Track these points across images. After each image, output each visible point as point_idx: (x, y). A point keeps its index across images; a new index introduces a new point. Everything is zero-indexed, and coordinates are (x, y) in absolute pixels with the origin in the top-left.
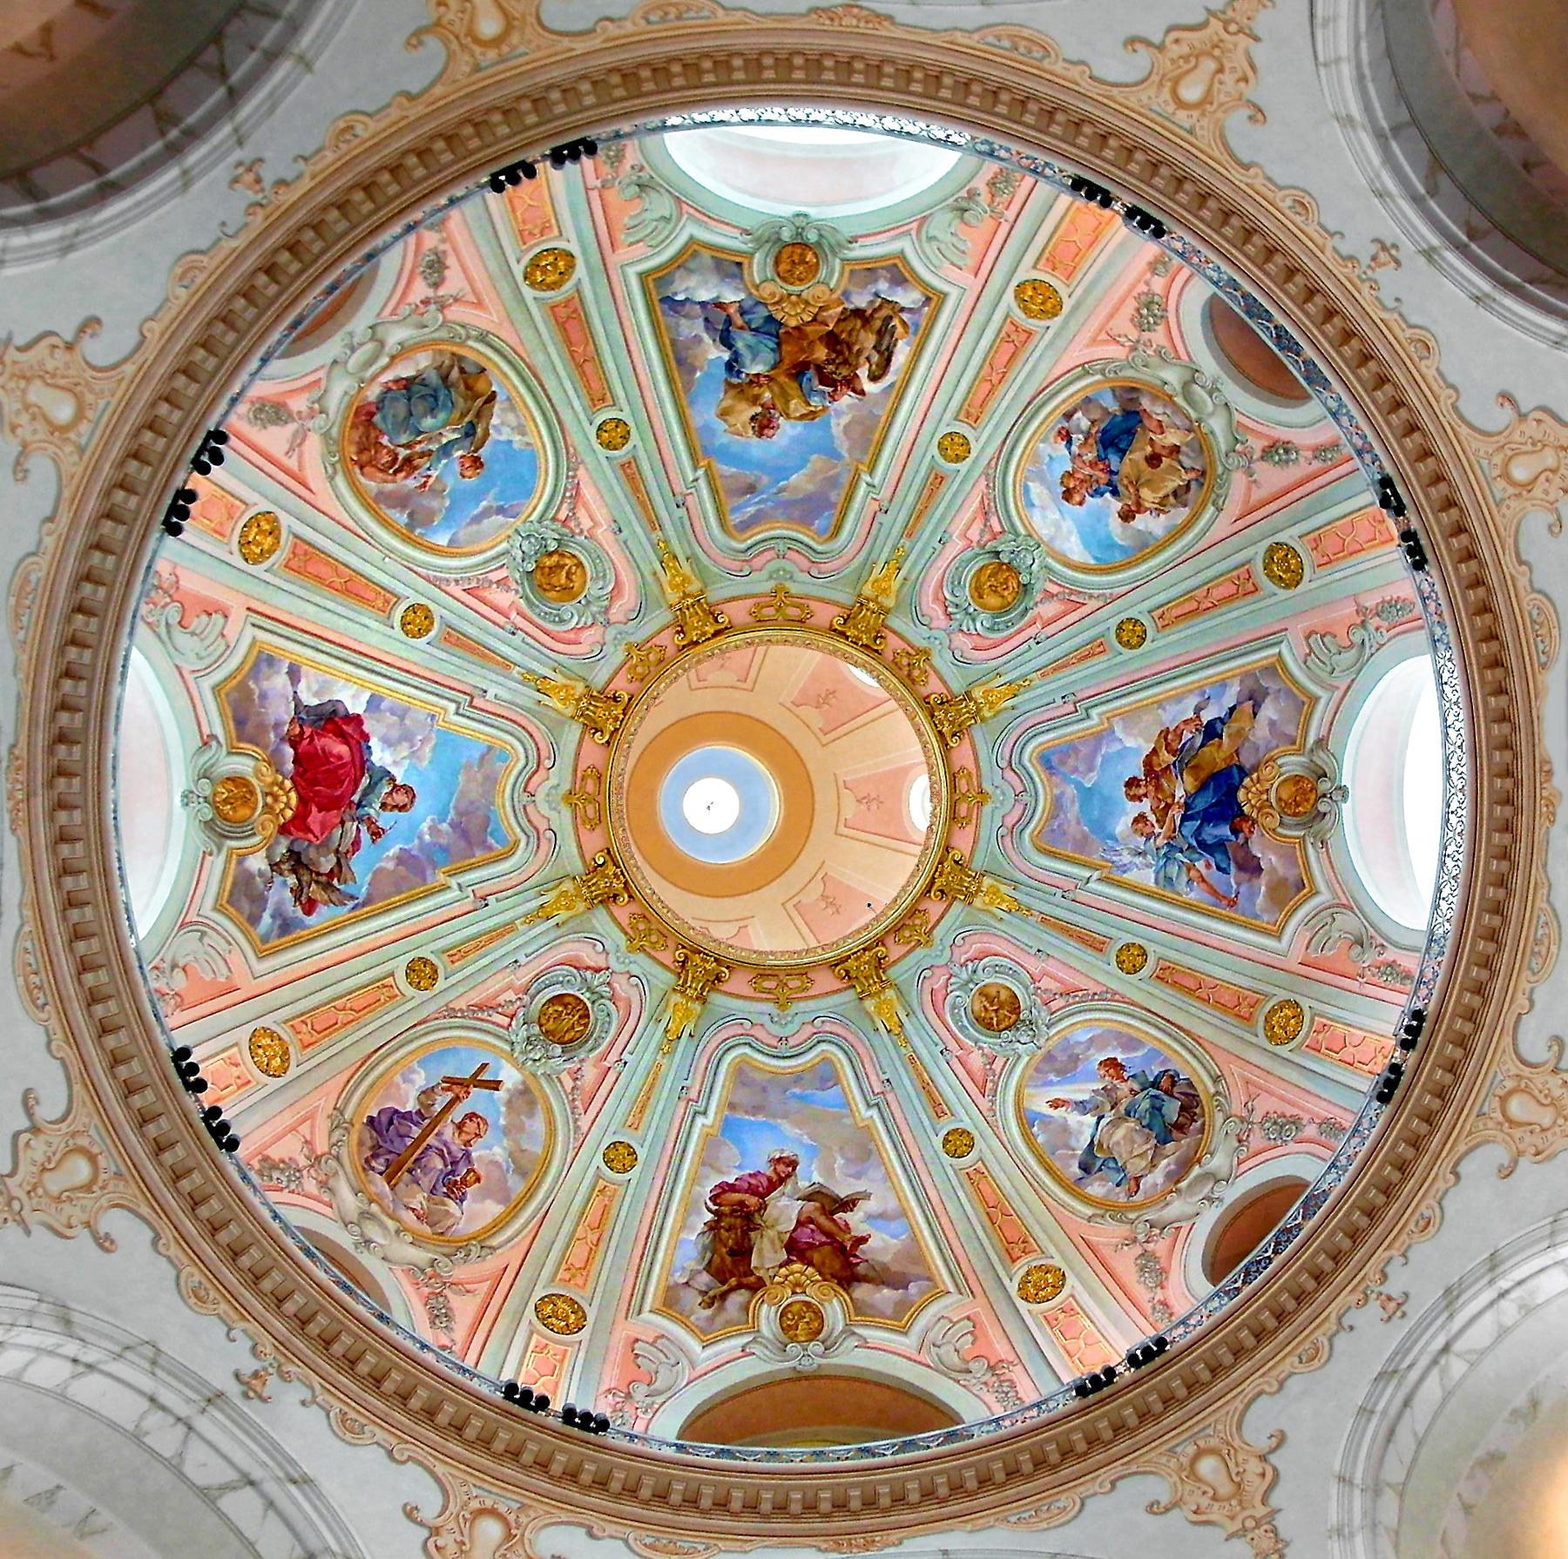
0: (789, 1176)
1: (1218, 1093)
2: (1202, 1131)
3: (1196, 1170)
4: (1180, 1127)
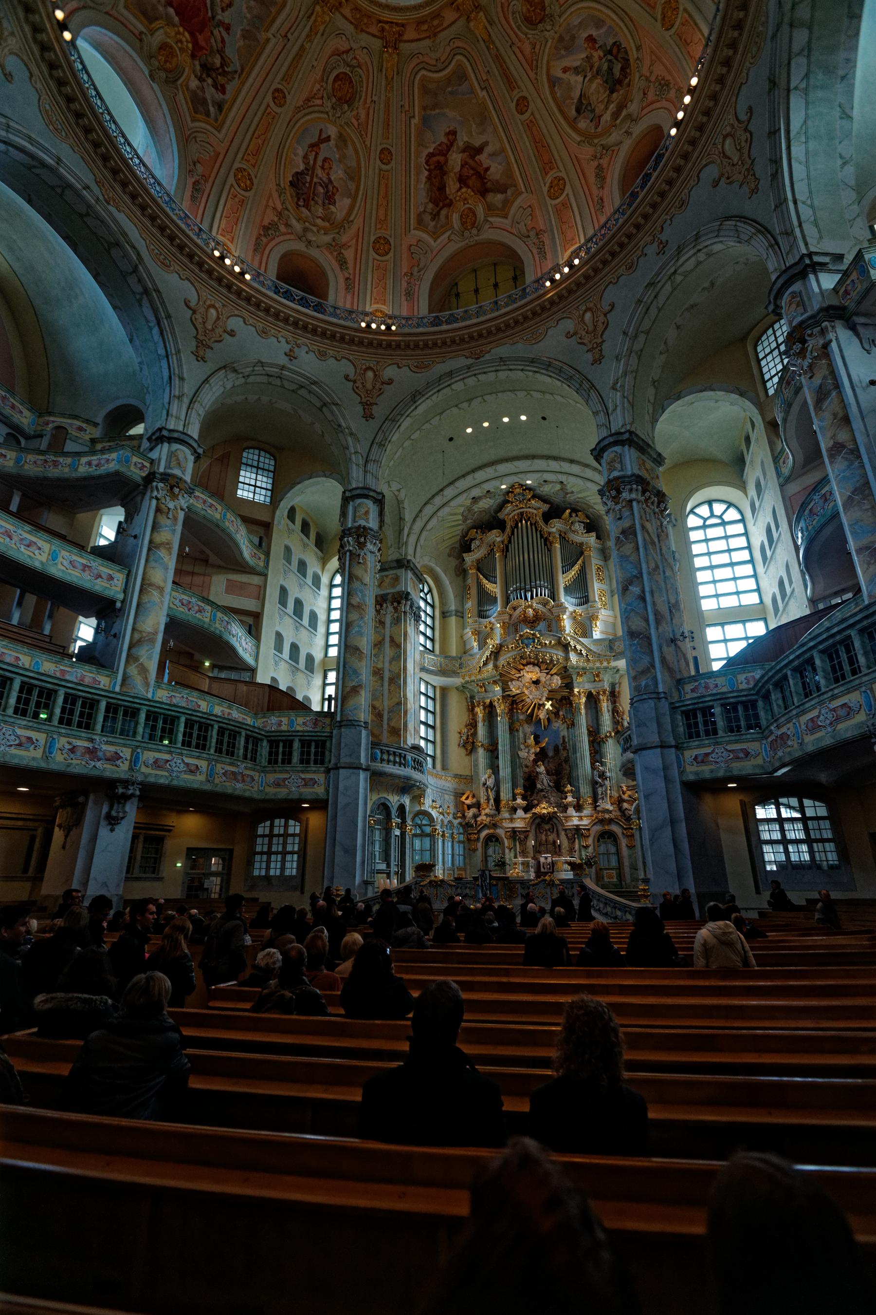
0: (455, 140)
1: (638, 59)
2: (629, 85)
3: (624, 113)
4: (620, 82)
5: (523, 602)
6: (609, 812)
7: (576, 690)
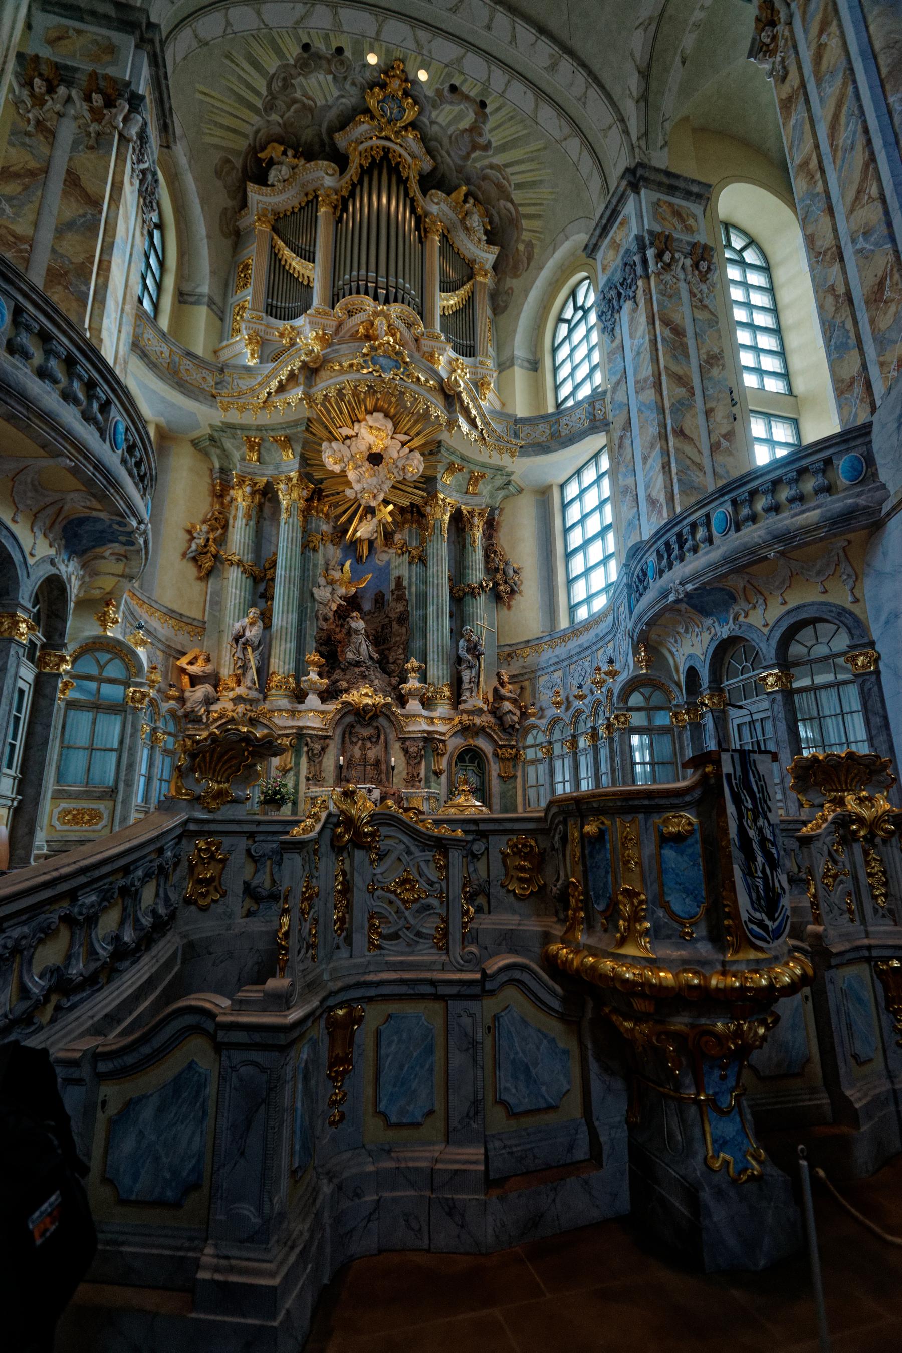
5: (369, 303)
6: (480, 711)
7: (441, 496)
